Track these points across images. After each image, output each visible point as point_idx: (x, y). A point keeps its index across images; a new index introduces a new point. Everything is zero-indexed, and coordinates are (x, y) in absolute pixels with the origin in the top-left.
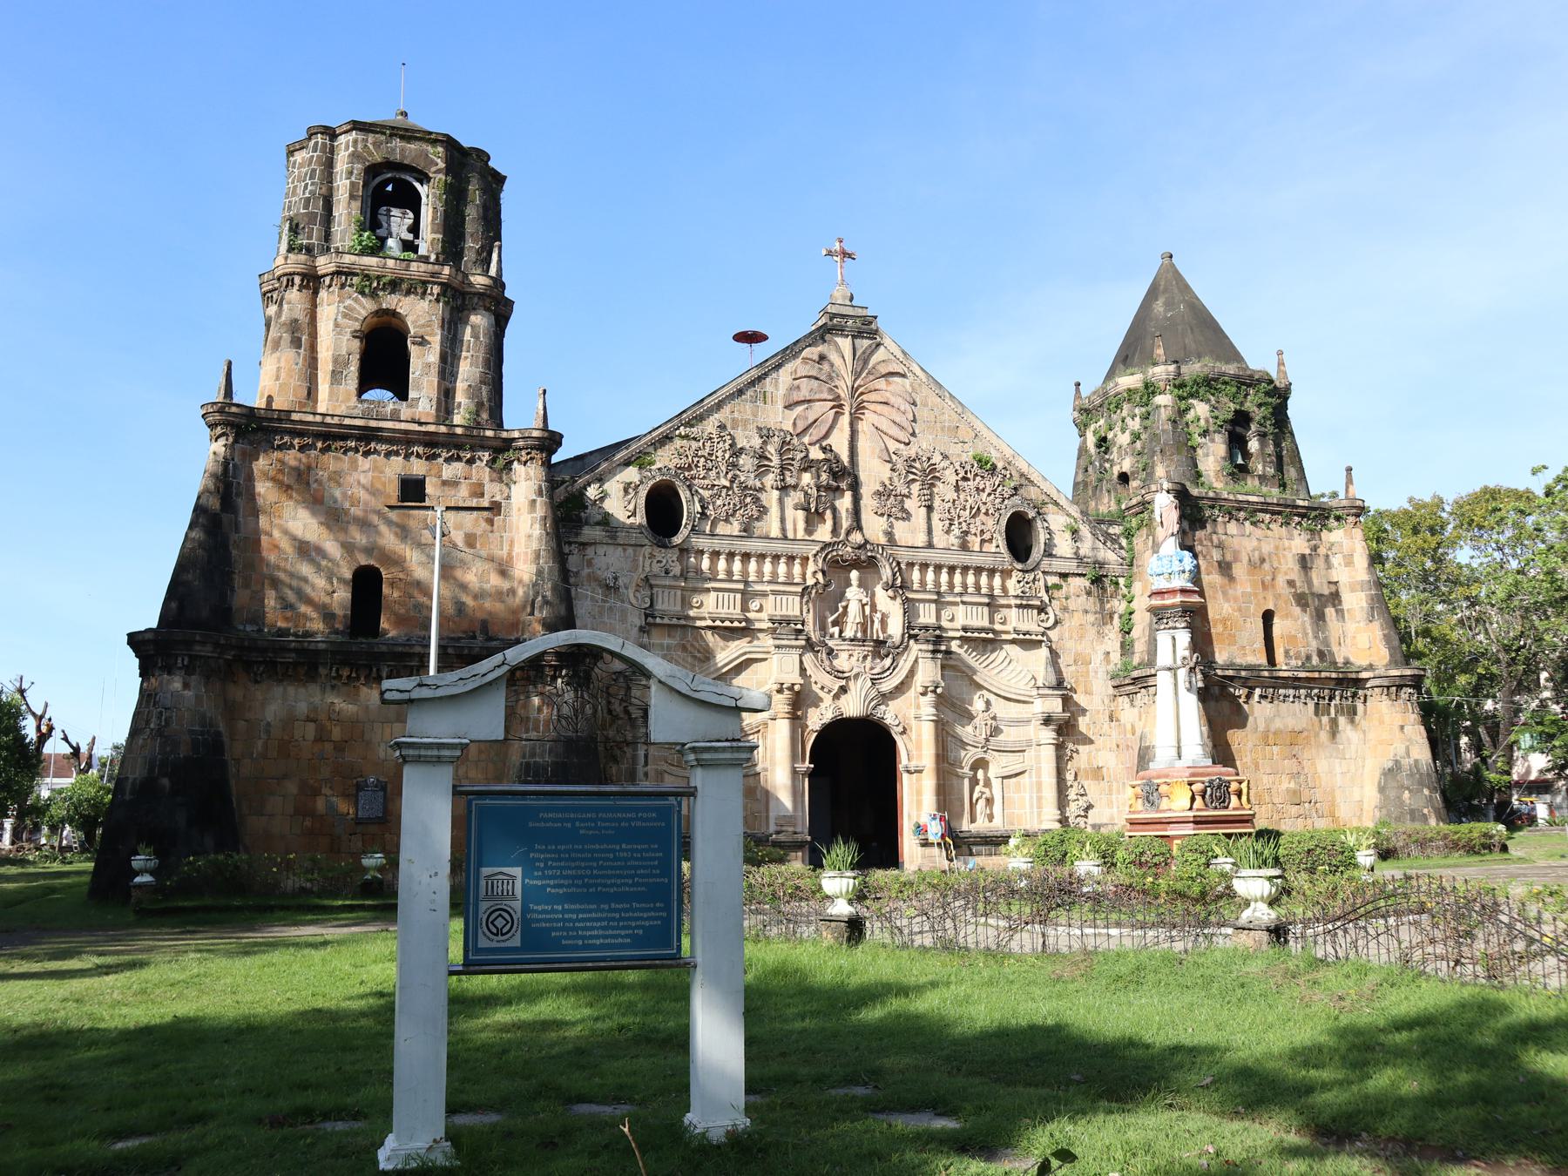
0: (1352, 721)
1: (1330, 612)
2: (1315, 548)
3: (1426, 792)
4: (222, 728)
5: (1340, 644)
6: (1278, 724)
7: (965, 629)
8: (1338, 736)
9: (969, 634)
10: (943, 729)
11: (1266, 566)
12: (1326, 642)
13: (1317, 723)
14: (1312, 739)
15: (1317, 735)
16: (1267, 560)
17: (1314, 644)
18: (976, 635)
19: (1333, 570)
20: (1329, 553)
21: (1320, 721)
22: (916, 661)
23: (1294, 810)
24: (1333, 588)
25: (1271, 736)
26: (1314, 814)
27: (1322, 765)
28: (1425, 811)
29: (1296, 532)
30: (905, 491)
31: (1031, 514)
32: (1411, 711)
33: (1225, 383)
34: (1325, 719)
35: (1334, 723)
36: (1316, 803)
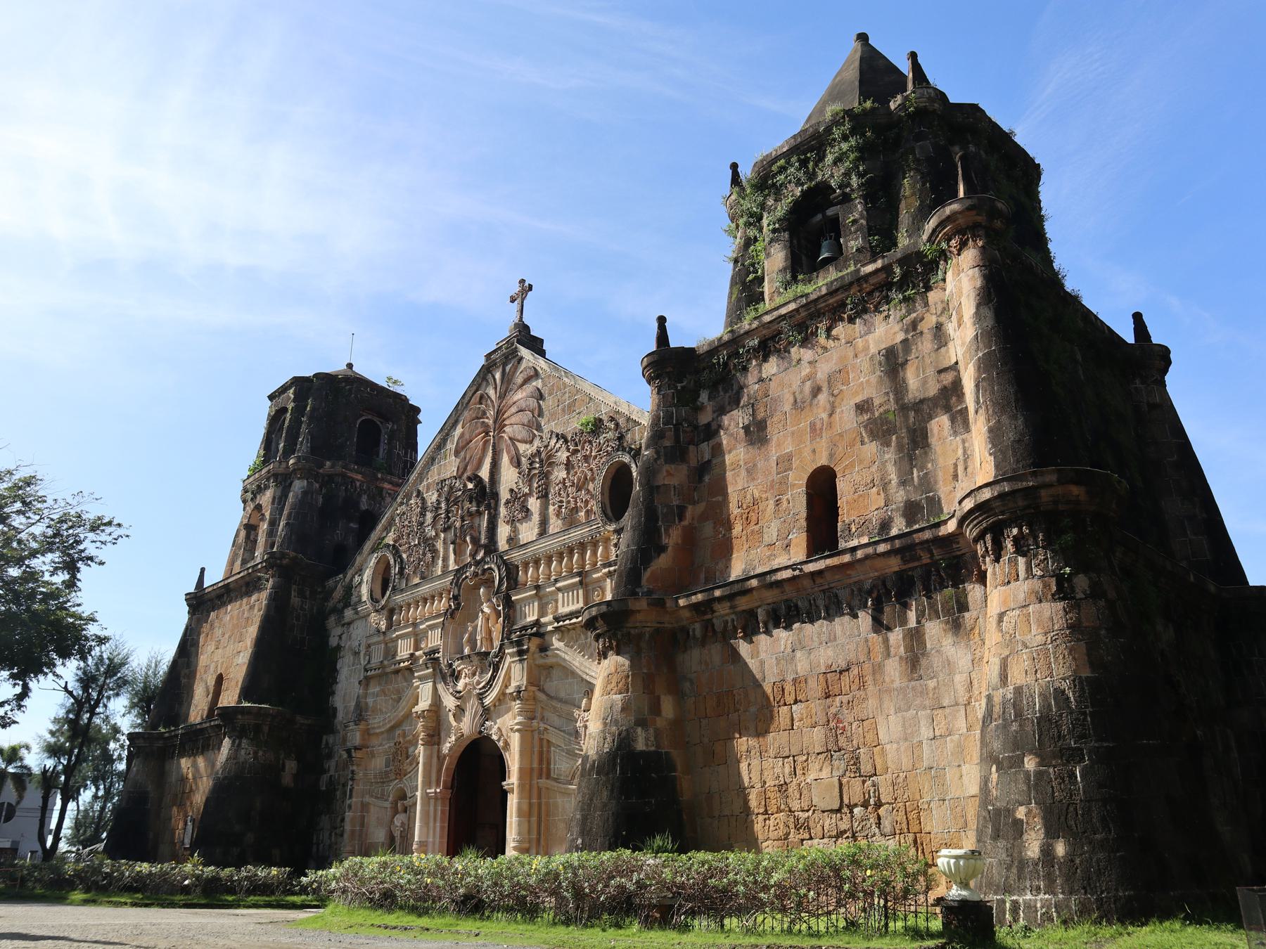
0: (956, 626)
1: (940, 425)
2: (914, 325)
3: (1030, 764)
4: (150, 788)
5: (955, 477)
6: (802, 664)
7: (557, 619)
8: (924, 662)
9: (561, 623)
10: (541, 740)
11: (822, 397)
12: (927, 483)
13: (878, 648)
14: (869, 679)
15: (878, 669)
16: (825, 389)
17: (900, 496)
18: (567, 622)
19: (951, 345)
20: (942, 319)
21: (886, 641)
22: (509, 667)
23: (829, 822)
24: (948, 378)
25: (789, 687)
26: (875, 829)
27: (889, 728)
28: (1021, 813)
29: (878, 319)
30: (527, 490)
31: (626, 459)
32: (1022, 574)
33: (782, 169)
34: (896, 636)
35: (915, 638)
36: (879, 805)
